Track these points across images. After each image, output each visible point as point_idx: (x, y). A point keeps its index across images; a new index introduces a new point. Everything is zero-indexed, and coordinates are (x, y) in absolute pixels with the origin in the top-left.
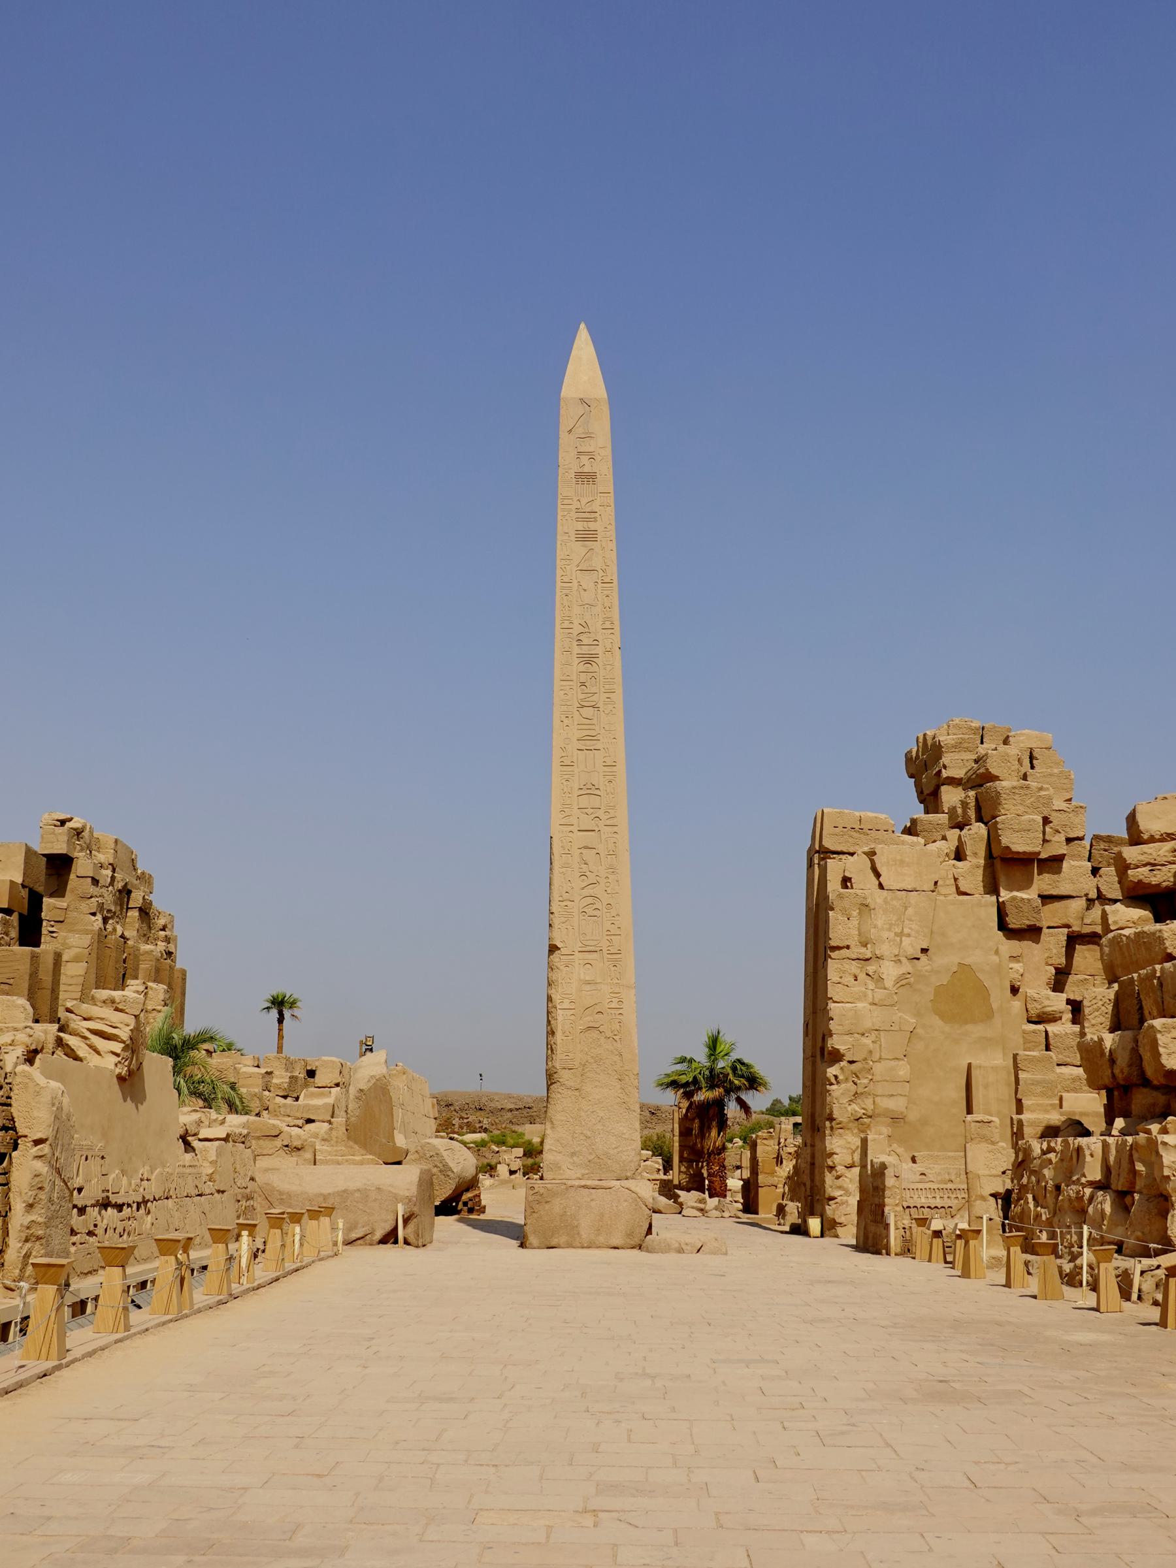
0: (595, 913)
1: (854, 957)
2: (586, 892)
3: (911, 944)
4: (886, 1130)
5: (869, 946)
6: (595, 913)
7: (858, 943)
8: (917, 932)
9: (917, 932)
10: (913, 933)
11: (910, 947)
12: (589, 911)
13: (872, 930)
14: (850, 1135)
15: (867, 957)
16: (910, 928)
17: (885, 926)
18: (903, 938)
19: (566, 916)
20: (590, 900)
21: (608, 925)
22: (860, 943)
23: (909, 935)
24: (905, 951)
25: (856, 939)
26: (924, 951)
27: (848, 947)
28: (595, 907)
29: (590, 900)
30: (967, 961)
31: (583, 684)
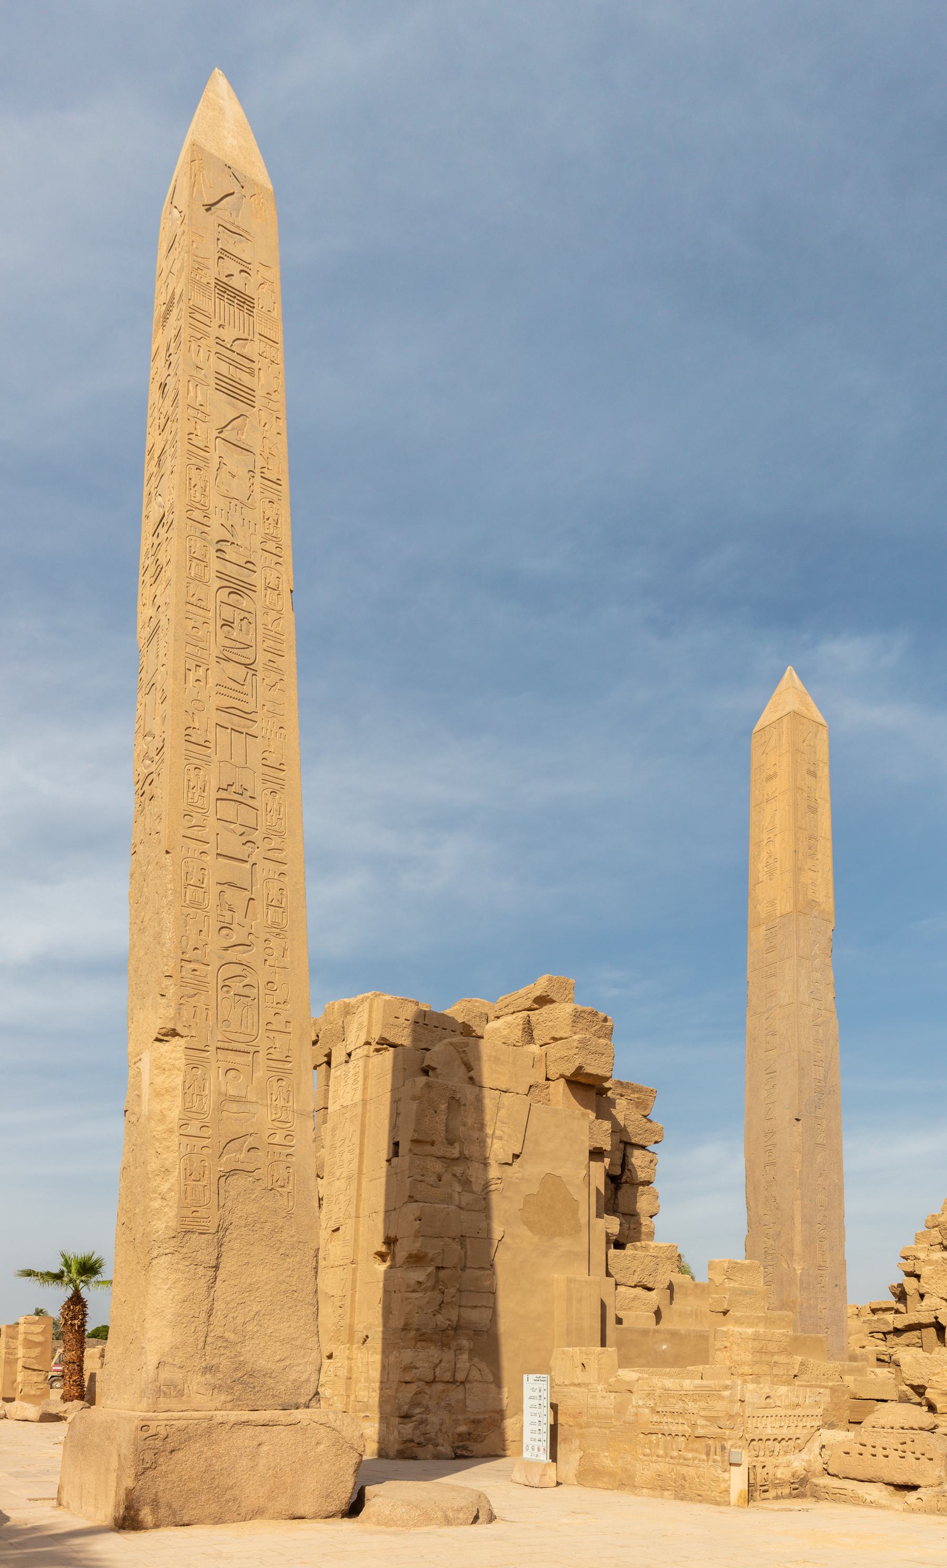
0: (247, 991)
1: (439, 1154)
2: (231, 955)
3: (503, 1148)
4: (467, 1343)
5: (456, 1145)
6: (247, 991)
7: (444, 1140)
8: (510, 1136)
9: (510, 1136)
10: (505, 1137)
11: (502, 1150)
12: (237, 986)
13: (462, 1128)
14: (432, 1348)
15: (454, 1156)
16: (502, 1131)
17: (475, 1125)
18: (495, 1141)
19: (194, 986)
20: (237, 970)
21: (267, 1016)
22: (447, 1140)
23: (501, 1138)
24: (496, 1154)
25: (443, 1135)
26: (516, 1156)
27: (433, 1144)
28: (246, 981)
29: (237, 970)
30: (558, 1172)
31: (227, 624)
